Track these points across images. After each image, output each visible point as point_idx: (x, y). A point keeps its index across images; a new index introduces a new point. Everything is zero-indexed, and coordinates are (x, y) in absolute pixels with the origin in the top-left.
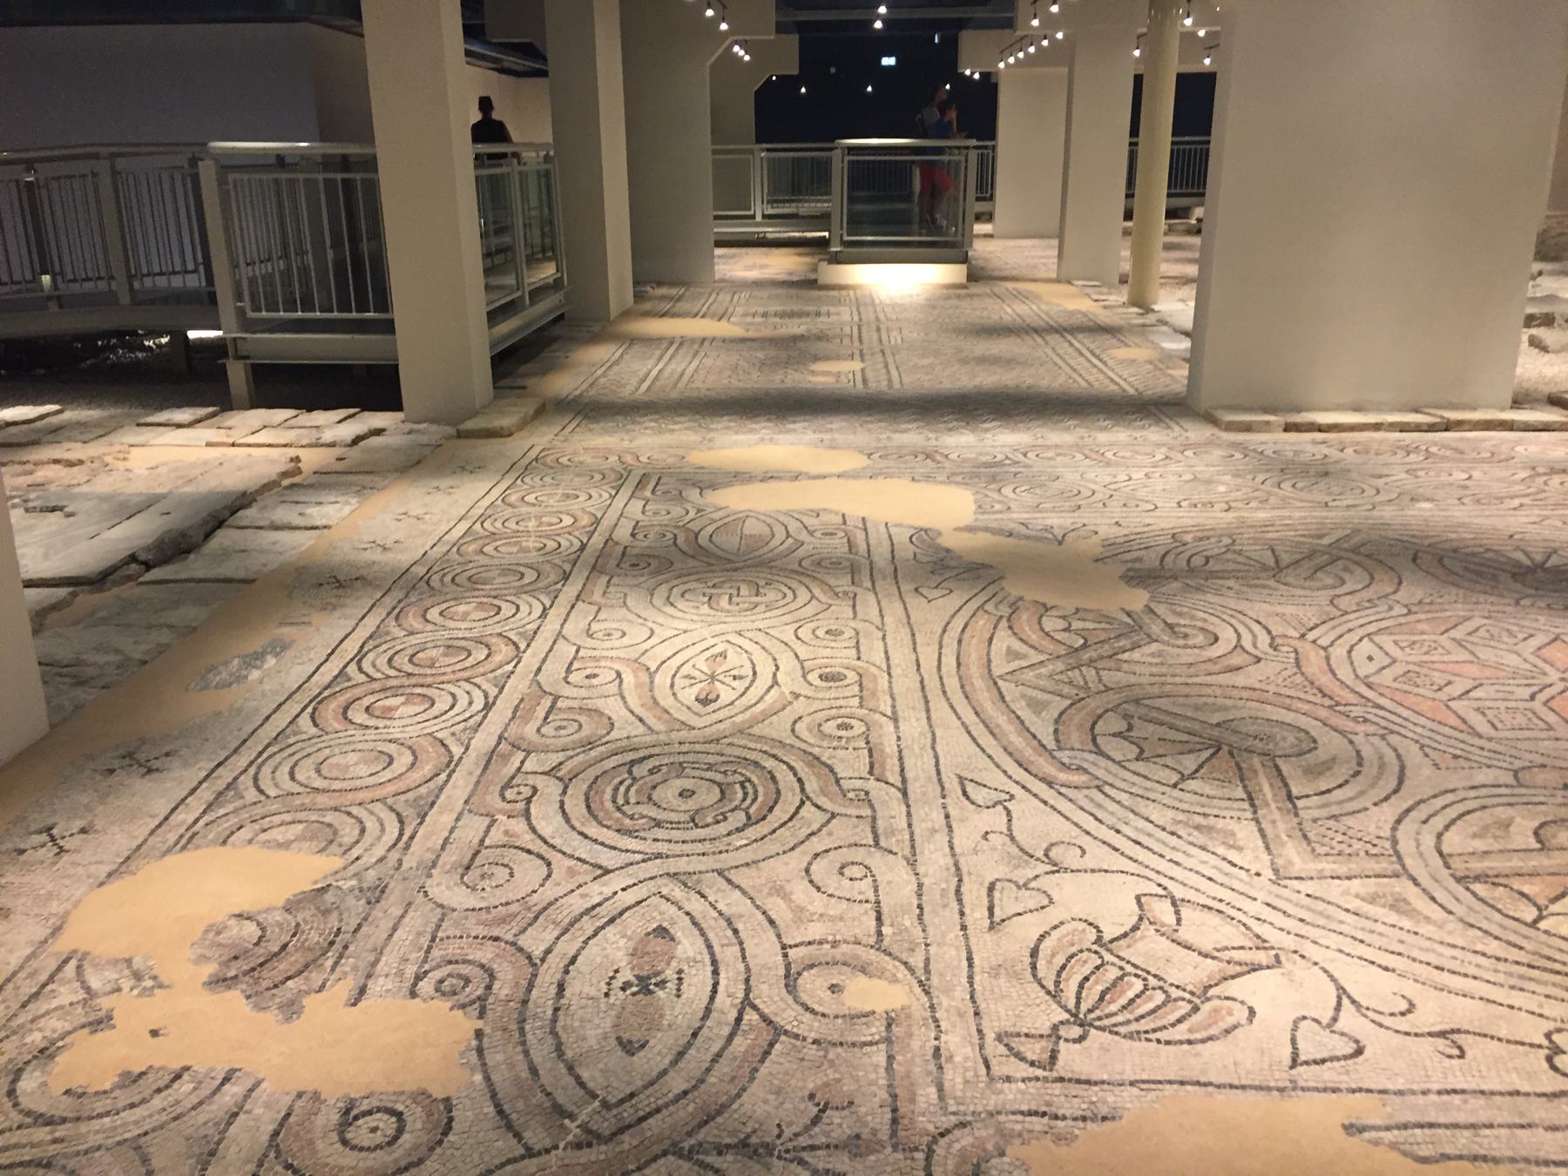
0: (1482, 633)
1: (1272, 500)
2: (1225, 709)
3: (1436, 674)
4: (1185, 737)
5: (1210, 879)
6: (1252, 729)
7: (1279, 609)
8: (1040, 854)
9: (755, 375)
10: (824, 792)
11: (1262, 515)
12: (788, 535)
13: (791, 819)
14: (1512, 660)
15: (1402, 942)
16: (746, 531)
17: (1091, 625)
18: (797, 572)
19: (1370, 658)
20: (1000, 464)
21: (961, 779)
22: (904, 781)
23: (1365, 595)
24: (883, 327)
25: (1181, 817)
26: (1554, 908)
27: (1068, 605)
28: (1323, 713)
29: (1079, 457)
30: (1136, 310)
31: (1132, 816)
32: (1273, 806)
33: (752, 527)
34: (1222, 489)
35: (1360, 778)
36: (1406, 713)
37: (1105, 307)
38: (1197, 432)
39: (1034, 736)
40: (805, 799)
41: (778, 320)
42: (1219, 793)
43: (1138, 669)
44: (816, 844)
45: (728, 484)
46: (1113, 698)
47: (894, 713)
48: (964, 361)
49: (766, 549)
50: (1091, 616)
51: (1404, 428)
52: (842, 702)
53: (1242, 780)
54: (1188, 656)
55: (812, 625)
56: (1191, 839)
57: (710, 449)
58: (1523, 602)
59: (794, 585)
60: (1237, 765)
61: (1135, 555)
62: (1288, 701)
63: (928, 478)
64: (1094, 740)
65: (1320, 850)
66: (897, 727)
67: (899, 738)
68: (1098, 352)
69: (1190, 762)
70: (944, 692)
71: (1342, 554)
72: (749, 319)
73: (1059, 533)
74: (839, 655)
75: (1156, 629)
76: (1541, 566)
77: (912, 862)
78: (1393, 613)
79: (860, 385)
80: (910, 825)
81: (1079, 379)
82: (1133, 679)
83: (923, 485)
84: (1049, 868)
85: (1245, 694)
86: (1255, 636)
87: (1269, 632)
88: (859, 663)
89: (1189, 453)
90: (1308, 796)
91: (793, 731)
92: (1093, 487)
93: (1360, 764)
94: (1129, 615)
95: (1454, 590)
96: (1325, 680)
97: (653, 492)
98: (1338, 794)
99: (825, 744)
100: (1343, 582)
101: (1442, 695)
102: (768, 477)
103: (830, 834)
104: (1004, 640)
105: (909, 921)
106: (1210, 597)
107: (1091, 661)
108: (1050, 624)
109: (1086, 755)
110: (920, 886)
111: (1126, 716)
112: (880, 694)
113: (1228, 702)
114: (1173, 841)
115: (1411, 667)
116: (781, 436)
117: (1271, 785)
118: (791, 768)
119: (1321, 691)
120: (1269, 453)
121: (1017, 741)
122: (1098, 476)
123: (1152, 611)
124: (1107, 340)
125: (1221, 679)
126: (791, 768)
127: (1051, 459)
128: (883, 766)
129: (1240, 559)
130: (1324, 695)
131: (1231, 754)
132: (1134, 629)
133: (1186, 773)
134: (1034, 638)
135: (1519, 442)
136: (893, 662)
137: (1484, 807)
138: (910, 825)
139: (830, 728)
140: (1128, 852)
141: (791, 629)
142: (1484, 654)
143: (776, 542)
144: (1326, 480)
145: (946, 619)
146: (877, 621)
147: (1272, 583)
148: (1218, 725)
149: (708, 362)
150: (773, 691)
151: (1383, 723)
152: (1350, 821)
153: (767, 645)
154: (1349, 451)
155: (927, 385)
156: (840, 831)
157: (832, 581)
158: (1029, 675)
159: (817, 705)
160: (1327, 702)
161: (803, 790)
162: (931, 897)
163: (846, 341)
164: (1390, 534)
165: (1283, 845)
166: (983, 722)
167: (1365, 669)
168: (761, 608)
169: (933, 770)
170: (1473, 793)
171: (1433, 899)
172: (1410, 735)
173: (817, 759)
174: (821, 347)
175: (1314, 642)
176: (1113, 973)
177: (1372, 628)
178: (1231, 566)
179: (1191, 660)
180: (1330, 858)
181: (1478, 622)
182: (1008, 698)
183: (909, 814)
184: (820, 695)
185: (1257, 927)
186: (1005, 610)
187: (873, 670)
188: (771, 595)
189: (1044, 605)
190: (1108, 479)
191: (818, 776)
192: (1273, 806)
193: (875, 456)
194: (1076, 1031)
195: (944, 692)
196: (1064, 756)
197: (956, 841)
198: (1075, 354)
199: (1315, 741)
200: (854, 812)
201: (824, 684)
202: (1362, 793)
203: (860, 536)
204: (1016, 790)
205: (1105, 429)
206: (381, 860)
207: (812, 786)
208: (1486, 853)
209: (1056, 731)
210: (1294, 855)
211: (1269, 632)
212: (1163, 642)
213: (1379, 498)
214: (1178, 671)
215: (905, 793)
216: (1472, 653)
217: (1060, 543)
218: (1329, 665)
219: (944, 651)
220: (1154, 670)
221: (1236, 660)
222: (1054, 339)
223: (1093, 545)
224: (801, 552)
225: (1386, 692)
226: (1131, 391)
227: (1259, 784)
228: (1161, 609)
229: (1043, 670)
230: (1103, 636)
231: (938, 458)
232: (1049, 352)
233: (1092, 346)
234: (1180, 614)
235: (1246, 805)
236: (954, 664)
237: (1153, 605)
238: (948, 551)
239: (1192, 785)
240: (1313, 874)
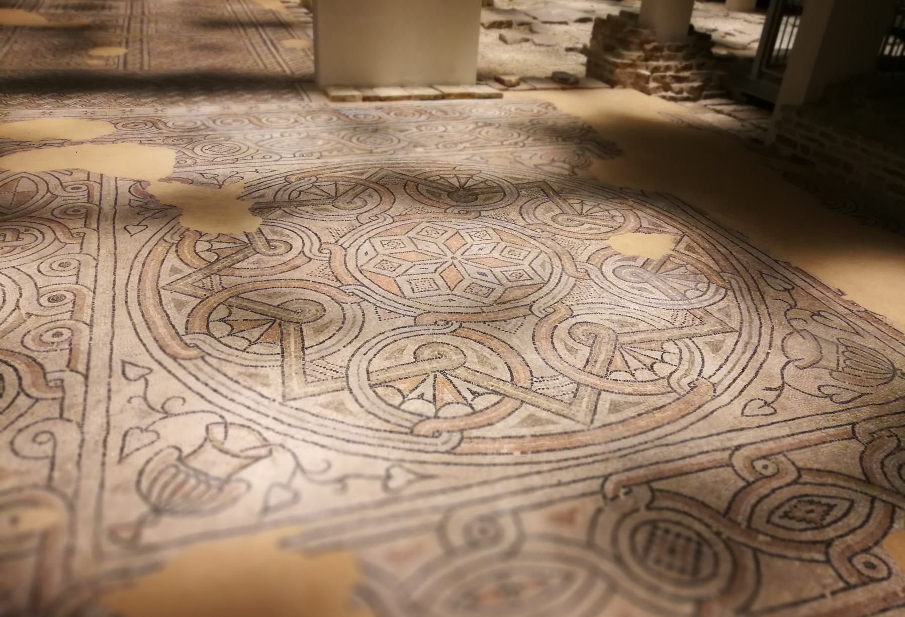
0: (424, 233)
1: (345, 150)
2: (285, 295)
3: (395, 260)
4: (257, 317)
5: (249, 408)
6: (293, 307)
7: (330, 225)
8: (158, 407)
9: (49, 59)
10: (34, 384)
11: (337, 160)
12: (48, 191)
13: (8, 407)
14: (433, 248)
15: (334, 429)
16: (18, 190)
17: (223, 245)
18: (49, 220)
19: (366, 253)
20: (197, 129)
21: (124, 363)
22: (88, 369)
23: (375, 212)
24: (145, 20)
25: (243, 369)
26: (411, 396)
27: (213, 231)
28: (334, 292)
29: (246, 122)
30: (304, 10)
31: (216, 373)
32: (293, 355)
33: (24, 186)
34: (320, 142)
35: (341, 331)
36: (373, 287)
37: (288, 7)
38: (316, 102)
39: (174, 327)
40: (21, 390)
41: (73, 12)
42: (267, 352)
43: (244, 273)
44: (22, 423)
45: (13, 151)
46: (226, 294)
47: (91, 321)
48: (193, 49)
49: (31, 202)
50: (225, 239)
52: (59, 317)
53: (281, 341)
54: (273, 261)
55: (51, 260)
56: (245, 384)
57: (5, 122)
58: (448, 211)
59: (44, 229)
60: (281, 330)
61: (261, 192)
62: (318, 286)
63: (151, 141)
64: (207, 326)
65: (310, 379)
66: (91, 331)
67: (91, 339)
68: (275, 42)
69: (256, 333)
70: (126, 302)
71: (372, 185)
72: (52, 11)
73: (220, 179)
74: (64, 282)
75: (260, 244)
76: (462, 187)
77: (81, 426)
78: (385, 223)
79: (121, 68)
80: (85, 400)
81: (260, 62)
82: (239, 280)
83: (146, 146)
84: (163, 415)
85: (297, 284)
86: (312, 244)
87: (320, 241)
88: (77, 286)
89: (309, 118)
90: (312, 347)
91: (22, 342)
92: (249, 144)
93: (343, 323)
94: (247, 236)
95: (418, 205)
96: (340, 270)
98: (328, 343)
99: (42, 349)
100: (366, 204)
101: (394, 274)
102: (43, 144)
103: (32, 414)
105: (71, 467)
106: (296, 220)
107: (219, 270)
108: (202, 246)
109: (202, 337)
110: (83, 440)
111: (230, 307)
112: (85, 308)
113: (287, 290)
114: (235, 386)
115: (386, 258)
116: (58, 111)
117: (296, 342)
118: (16, 370)
119: (336, 277)
120: (351, 116)
121: (163, 331)
122: (254, 135)
123: (261, 232)
124: (282, 32)
125: (286, 275)
126: (16, 370)
127: (229, 124)
128: (77, 361)
129: (319, 192)
130: (338, 280)
131: (280, 325)
132: (246, 246)
133: (253, 340)
134: (188, 256)
135: (475, 106)
136: (99, 283)
137: (396, 341)
138: (85, 400)
139: (47, 337)
140: (209, 398)
141: (35, 265)
142: (422, 245)
143: (38, 197)
144: (377, 135)
145: (139, 248)
146: (94, 254)
147: (330, 207)
148: (278, 306)
149: (16, 47)
150: (17, 310)
151: (361, 295)
152: (328, 359)
153: (16, 278)
154: (392, 114)
155: (165, 67)
156: (41, 410)
157: (71, 226)
158: (180, 285)
159: (43, 320)
160: (338, 284)
161: (20, 385)
162: (89, 445)
163: (118, 31)
164: (398, 170)
165: (291, 379)
166: (145, 320)
167: (362, 260)
168: (18, 250)
169: (107, 359)
170: (392, 333)
171: (357, 400)
172: (372, 300)
173: (35, 360)
174: (101, 35)
175: (341, 246)
176: (181, 477)
177: (372, 234)
178: (312, 197)
179: (274, 264)
180: (314, 384)
181: (424, 224)
182: (164, 303)
183: (86, 392)
184: (45, 314)
185: (266, 434)
186: (176, 238)
187: (85, 290)
188: (27, 239)
189: (200, 233)
190: (259, 138)
191: (32, 372)
192: (293, 355)
193: (119, 126)
195: (126, 302)
196: (187, 339)
197: (111, 407)
198: (262, 44)
199: (325, 311)
200: (50, 396)
201: (51, 304)
202: (340, 340)
203: (97, 187)
204: (155, 366)
205: (266, 101)
207: (27, 381)
208: (388, 368)
209: (187, 322)
210: (296, 386)
211: (320, 241)
212: (264, 254)
213: (400, 146)
214: (265, 272)
215: (86, 377)
216: (416, 245)
217: (221, 187)
218: (345, 260)
219: (132, 272)
220: (252, 273)
221: (298, 262)
222: (252, 32)
223: (236, 188)
224: (53, 205)
225: (368, 274)
226: (288, 72)
227: (289, 343)
228: (266, 230)
229: (189, 280)
230: (229, 252)
231: (160, 126)
232: (247, 42)
233: (272, 38)
234: (274, 232)
235: (279, 357)
236: (137, 281)
237: (262, 228)
238: (151, 196)
239: (255, 348)
240: (302, 395)
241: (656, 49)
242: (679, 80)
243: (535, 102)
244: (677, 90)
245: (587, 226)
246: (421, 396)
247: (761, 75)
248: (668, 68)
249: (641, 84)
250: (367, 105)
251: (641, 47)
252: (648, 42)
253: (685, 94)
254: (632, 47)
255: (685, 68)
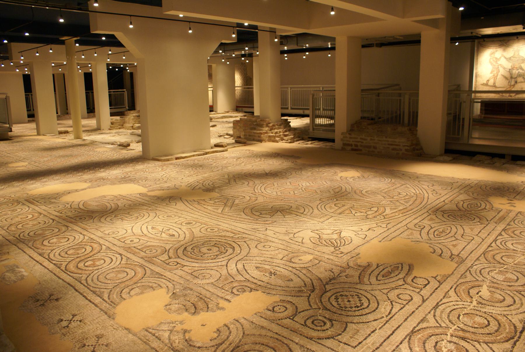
38: (160, 163)
51: (199, 155)
97: (40, 203)
104: (209, 208)
125: (257, 202)
193: (88, 182)
194: (337, 249)
206: (173, 285)
241: (273, 125)
242: (285, 136)
243: (243, 150)
244: (287, 139)
245: (325, 174)
246: (356, 213)
247: (313, 129)
248: (280, 132)
249: (272, 139)
250: (178, 160)
251: (267, 126)
252: (270, 123)
253: (290, 141)
254: (264, 126)
255: (286, 131)
